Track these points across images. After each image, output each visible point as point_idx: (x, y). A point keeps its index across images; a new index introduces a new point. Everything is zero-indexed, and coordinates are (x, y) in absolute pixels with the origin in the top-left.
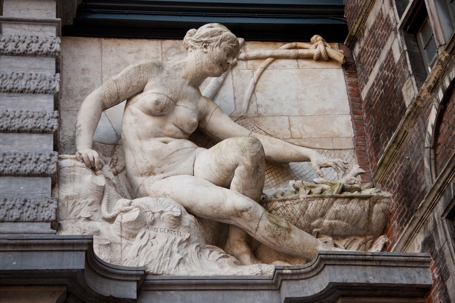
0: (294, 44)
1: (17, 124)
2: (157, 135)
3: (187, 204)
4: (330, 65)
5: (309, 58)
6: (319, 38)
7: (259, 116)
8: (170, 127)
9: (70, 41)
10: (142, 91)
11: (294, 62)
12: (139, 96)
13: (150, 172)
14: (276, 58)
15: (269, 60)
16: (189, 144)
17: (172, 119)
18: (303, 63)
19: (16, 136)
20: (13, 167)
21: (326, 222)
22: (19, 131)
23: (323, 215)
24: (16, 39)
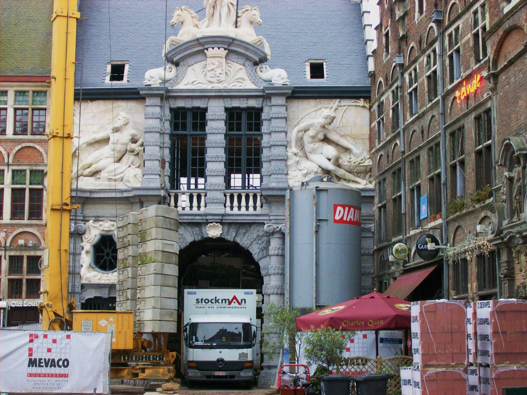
2: (312, 143)
5: (359, 106)
7: (343, 127)
8: (317, 140)
9: (289, 100)
10: (308, 130)
11: (355, 107)
12: (308, 131)
13: (311, 153)
14: (349, 106)
15: (347, 107)
16: (320, 144)
18: (357, 107)
19: (276, 147)
20: (276, 158)
22: (277, 146)
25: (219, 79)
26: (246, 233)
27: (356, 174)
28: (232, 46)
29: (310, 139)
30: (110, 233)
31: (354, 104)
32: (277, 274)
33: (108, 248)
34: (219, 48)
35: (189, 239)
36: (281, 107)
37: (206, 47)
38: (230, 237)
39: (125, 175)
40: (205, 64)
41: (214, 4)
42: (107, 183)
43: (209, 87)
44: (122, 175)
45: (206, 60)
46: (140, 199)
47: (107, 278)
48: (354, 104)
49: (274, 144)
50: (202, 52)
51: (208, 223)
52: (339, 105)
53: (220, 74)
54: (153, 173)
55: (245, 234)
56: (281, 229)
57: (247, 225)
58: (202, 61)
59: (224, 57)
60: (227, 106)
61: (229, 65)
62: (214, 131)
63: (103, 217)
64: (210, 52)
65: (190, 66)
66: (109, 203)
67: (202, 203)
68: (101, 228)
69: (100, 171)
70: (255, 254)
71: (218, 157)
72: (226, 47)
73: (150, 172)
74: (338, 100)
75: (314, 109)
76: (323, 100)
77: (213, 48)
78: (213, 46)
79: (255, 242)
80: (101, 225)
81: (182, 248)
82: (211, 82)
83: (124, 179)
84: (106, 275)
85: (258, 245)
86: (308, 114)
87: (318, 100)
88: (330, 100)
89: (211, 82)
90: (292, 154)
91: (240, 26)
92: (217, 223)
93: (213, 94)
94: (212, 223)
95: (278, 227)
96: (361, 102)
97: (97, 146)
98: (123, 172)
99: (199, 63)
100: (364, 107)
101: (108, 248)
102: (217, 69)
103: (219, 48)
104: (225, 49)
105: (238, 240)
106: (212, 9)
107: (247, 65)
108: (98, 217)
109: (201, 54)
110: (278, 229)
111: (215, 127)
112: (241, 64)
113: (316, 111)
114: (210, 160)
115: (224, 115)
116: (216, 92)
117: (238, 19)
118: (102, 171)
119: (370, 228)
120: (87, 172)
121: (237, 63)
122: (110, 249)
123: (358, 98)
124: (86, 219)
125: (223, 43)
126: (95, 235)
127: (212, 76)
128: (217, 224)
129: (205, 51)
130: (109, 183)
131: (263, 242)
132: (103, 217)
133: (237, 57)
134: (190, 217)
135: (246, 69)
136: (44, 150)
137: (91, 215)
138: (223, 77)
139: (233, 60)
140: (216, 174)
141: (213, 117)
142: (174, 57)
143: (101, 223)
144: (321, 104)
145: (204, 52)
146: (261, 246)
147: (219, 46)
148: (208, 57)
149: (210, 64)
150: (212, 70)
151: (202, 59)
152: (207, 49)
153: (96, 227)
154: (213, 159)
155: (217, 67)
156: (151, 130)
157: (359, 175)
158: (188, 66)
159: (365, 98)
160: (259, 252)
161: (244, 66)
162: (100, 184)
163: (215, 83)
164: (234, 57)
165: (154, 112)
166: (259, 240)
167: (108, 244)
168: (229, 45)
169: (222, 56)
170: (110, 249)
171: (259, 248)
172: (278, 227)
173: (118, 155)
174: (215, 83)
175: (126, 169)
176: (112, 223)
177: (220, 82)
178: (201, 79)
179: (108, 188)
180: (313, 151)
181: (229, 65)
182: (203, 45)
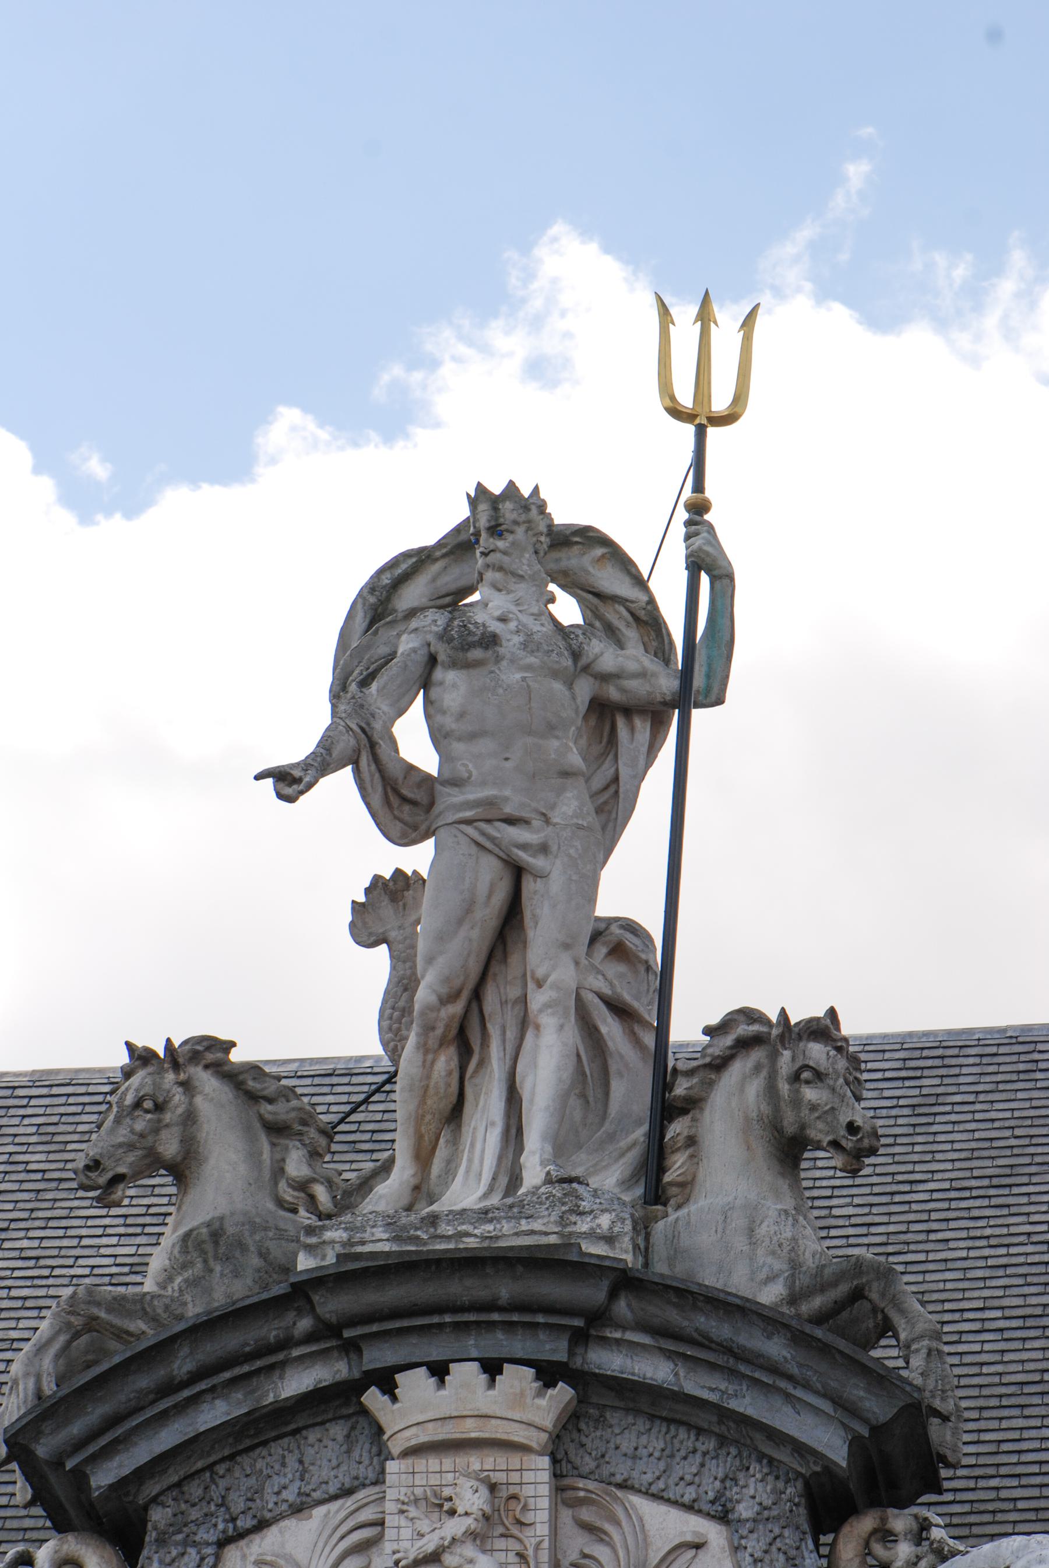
28: (604, 1341)
34: (492, 1368)
40: (367, 1514)
41: (457, 1008)
45: (379, 1480)
58: (347, 1492)
59: (536, 1439)
61: (586, 1514)
65: (241, 1535)
72: (555, 1350)
77: (439, 1371)
78: (436, 1353)
91: (687, 1185)
99: (319, 1512)
102: (469, 1550)
103: (492, 1368)
106: (445, 1062)
107: (745, 1510)
109: (338, 1430)
112: (690, 1507)
117: (677, 1128)
129: (373, 1398)
135: (736, 1549)
139: (621, 1470)
142: (94, 1458)
145: (364, 1412)
147: (498, 1344)
148: (396, 1447)
152: (388, 1385)
155: (472, 1535)
158: (222, 1544)
161: (723, 1517)
164: (627, 1442)
168: (580, 1338)
169: (519, 1435)
181: (586, 1514)
182: (352, 1348)
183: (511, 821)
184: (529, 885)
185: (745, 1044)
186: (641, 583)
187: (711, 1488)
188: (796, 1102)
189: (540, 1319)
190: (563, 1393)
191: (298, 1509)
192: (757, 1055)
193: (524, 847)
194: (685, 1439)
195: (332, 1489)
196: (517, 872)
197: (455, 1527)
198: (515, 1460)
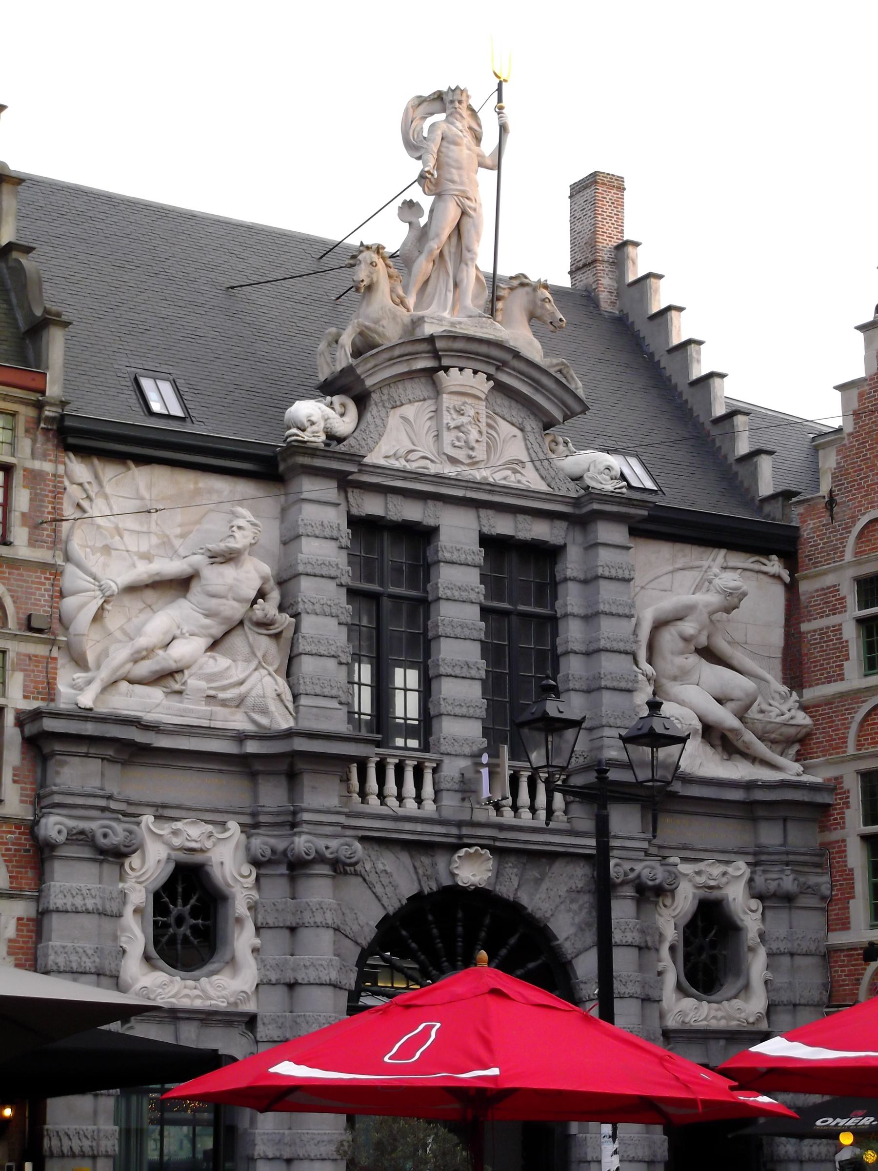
0: (757, 558)
1: (616, 646)
2: (682, 653)
3: (699, 714)
4: (776, 581)
5: (765, 573)
6: (777, 558)
10: (680, 619)
11: (755, 575)
12: (679, 623)
13: (675, 679)
17: (693, 642)
18: (761, 576)
21: (773, 736)
23: (773, 732)
24: (610, 565)
25: (473, 454)
26: (542, 880)
27: (769, 744)
29: (681, 644)
30: (198, 858)
31: (757, 567)
32: (631, 997)
33: (180, 901)
34: (475, 372)
35: (407, 888)
36: (618, 551)
37: (445, 362)
38: (506, 889)
39: (251, 689)
42: (204, 708)
43: (450, 470)
44: (243, 689)
46: (291, 765)
47: (197, 992)
48: (757, 567)
49: (608, 646)
50: (430, 373)
51: (456, 848)
52: (725, 565)
53: (477, 441)
54: (326, 691)
55: (538, 882)
56: (639, 876)
57: (544, 860)
58: (424, 400)
59: (483, 396)
60: (485, 530)
62: (457, 594)
63: (178, 807)
64: (454, 379)
66: (190, 768)
67: (428, 790)
68: (177, 842)
69: (180, 671)
70: (567, 939)
71: (469, 667)
73: (318, 690)
74: (723, 552)
75: (670, 568)
76: (689, 546)
77: (461, 369)
79: (562, 907)
80: (175, 833)
81: (391, 913)
82: (453, 461)
83: (250, 701)
84: (190, 983)
85: (571, 914)
86: (656, 578)
87: (678, 546)
88: (702, 549)
89: (453, 461)
90: (645, 679)
92: (483, 847)
93: (460, 493)
94: (469, 846)
95: (632, 870)
96: (774, 565)
97: (150, 596)
98: (241, 683)
99: (416, 404)
100: (777, 577)
101: (180, 901)
103: (475, 372)
104: (489, 377)
105: (524, 900)
108: (164, 806)
110: (632, 876)
111: (459, 584)
112: (513, 424)
113: (672, 572)
114: (449, 671)
115: (478, 555)
116: (466, 488)
118: (186, 672)
119: (818, 885)
120: (144, 669)
121: (504, 419)
122: (185, 904)
123: (765, 552)
124: (132, 810)
125: (487, 359)
126: (159, 861)
127: (457, 444)
128: (483, 852)
129: (442, 373)
130: (209, 708)
131: (581, 908)
132: (178, 807)
133: (506, 402)
134: (419, 827)
136: (9, 590)
137: (144, 799)
138: (480, 453)
139: (498, 410)
140: (464, 711)
141: (455, 557)
143: (178, 825)
144: (684, 556)
146: (577, 920)
149: (452, 411)
150: (457, 428)
151: (426, 394)
152: (446, 369)
153: (161, 836)
154: (457, 671)
156: (317, 571)
157: (774, 746)
159: (781, 555)
160: (575, 935)
161: (522, 430)
162: (185, 710)
163: (463, 463)
164: (499, 401)
165: (326, 523)
166: (572, 901)
167: (180, 890)
170: (185, 904)
171: (573, 924)
172: (632, 870)
173: (217, 630)
174: (463, 463)
175: (250, 675)
176: (210, 828)
177: (474, 463)
178: (427, 447)
179: (205, 723)
180: (681, 676)
183: (468, 198)
184: (466, 220)
185: (523, 285)
186: (480, 126)
187: (520, 420)
188: (543, 307)
189: (492, 361)
190: (491, 383)
191: (410, 402)
192: (527, 289)
193: (470, 208)
194: (513, 404)
195: (422, 398)
196: (464, 213)
197: (464, 419)
198: (477, 402)
